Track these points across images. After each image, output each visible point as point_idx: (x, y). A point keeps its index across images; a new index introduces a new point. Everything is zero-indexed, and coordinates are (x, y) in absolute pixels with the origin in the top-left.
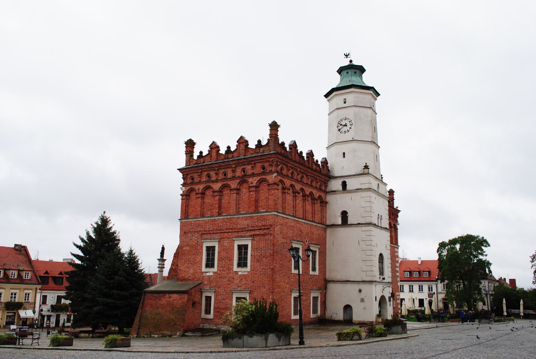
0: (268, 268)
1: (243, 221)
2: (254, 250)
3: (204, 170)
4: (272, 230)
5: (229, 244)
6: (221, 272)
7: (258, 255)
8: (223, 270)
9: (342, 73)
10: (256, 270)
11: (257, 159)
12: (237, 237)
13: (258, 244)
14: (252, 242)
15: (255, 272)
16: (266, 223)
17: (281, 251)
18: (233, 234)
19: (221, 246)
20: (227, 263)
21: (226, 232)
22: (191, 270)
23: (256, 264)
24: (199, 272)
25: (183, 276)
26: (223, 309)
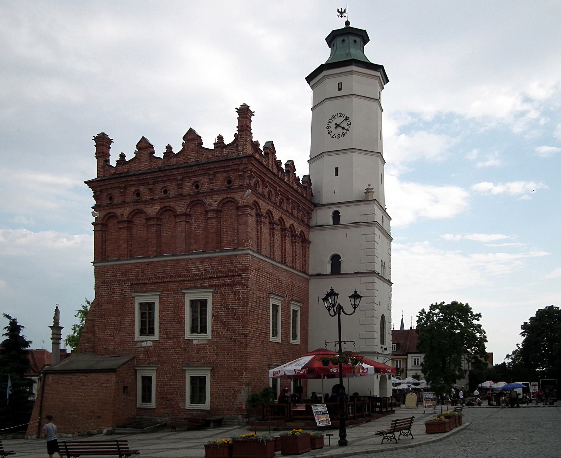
0: (239, 334)
1: (197, 265)
4: (245, 278)
5: (176, 299)
7: (223, 316)
8: (169, 338)
9: (334, 42)
10: (220, 337)
12: (189, 288)
13: (223, 299)
14: (213, 295)
15: (219, 340)
16: (235, 267)
17: (256, 308)
18: (182, 284)
19: (164, 302)
20: (175, 327)
21: (170, 282)
22: (116, 339)
23: (221, 328)
24: (130, 341)
26: (171, 395)
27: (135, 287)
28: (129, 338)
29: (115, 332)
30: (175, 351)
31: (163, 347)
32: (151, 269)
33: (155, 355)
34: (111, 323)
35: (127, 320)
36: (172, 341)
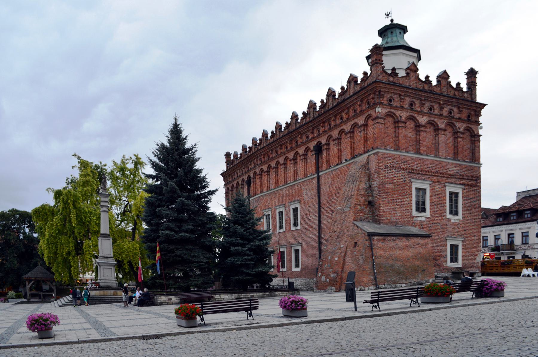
25: (388, 218)
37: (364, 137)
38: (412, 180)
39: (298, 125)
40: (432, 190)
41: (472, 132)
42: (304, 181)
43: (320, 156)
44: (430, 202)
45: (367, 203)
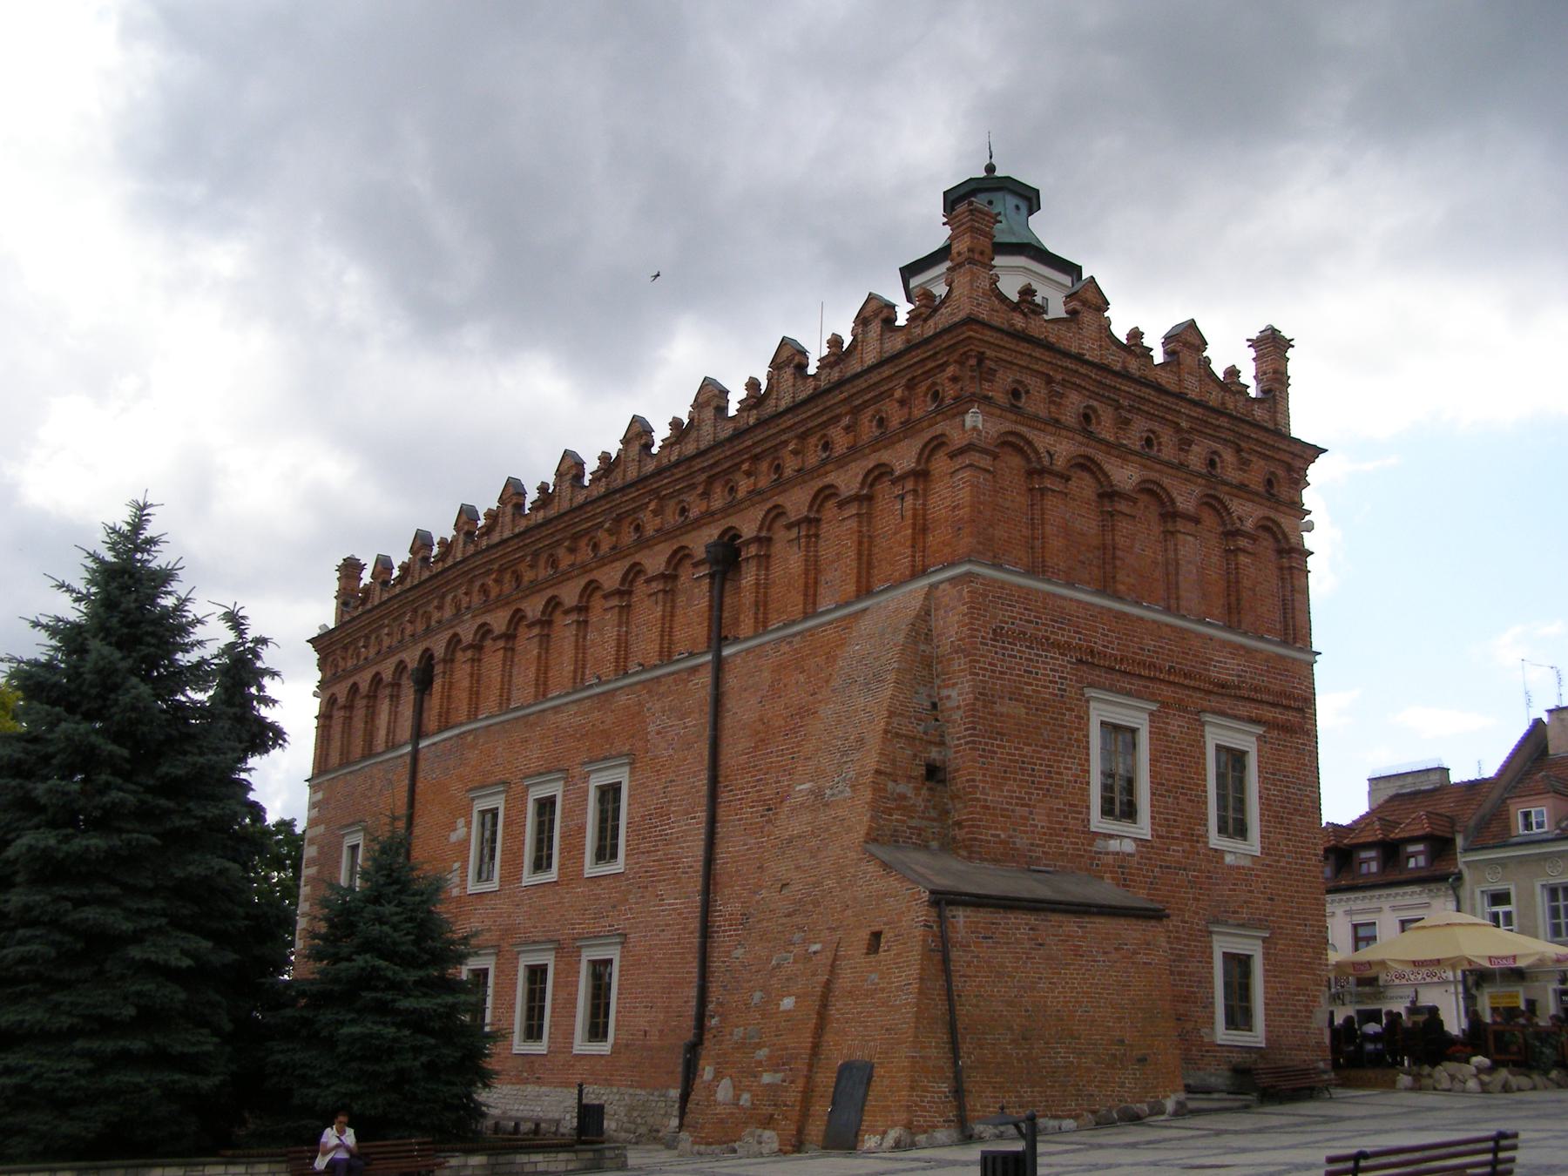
1: (1224, 657)
2: (1265, 778)
3: (1075, 384)
6: (1165, 843)
7: (1280, 801)
8: (1173, 838)
10: (1275, 855)
11: (1264, 439)
20: (1184, 811)
24: (1077, 831)
25: (1003, 836)
26: (1183, 1002)
27: (1084, 672)
28: (1073, 818)
29: (1033, 794)
30: (1187, 875)
31: (1161, 860)
32: (1124, 634)
33: (1141, 882)
34: (1023, 762)
35: (1067, 763)
36: (1180, 849)
37: (915, 516)
38: (1090, 692)
39: (650, 467)
40: (1157, 734)
41: (1280, 536)
42: (657, 678)
43: (728, 586)
44: (1151, 782)
45: (923, 771)
